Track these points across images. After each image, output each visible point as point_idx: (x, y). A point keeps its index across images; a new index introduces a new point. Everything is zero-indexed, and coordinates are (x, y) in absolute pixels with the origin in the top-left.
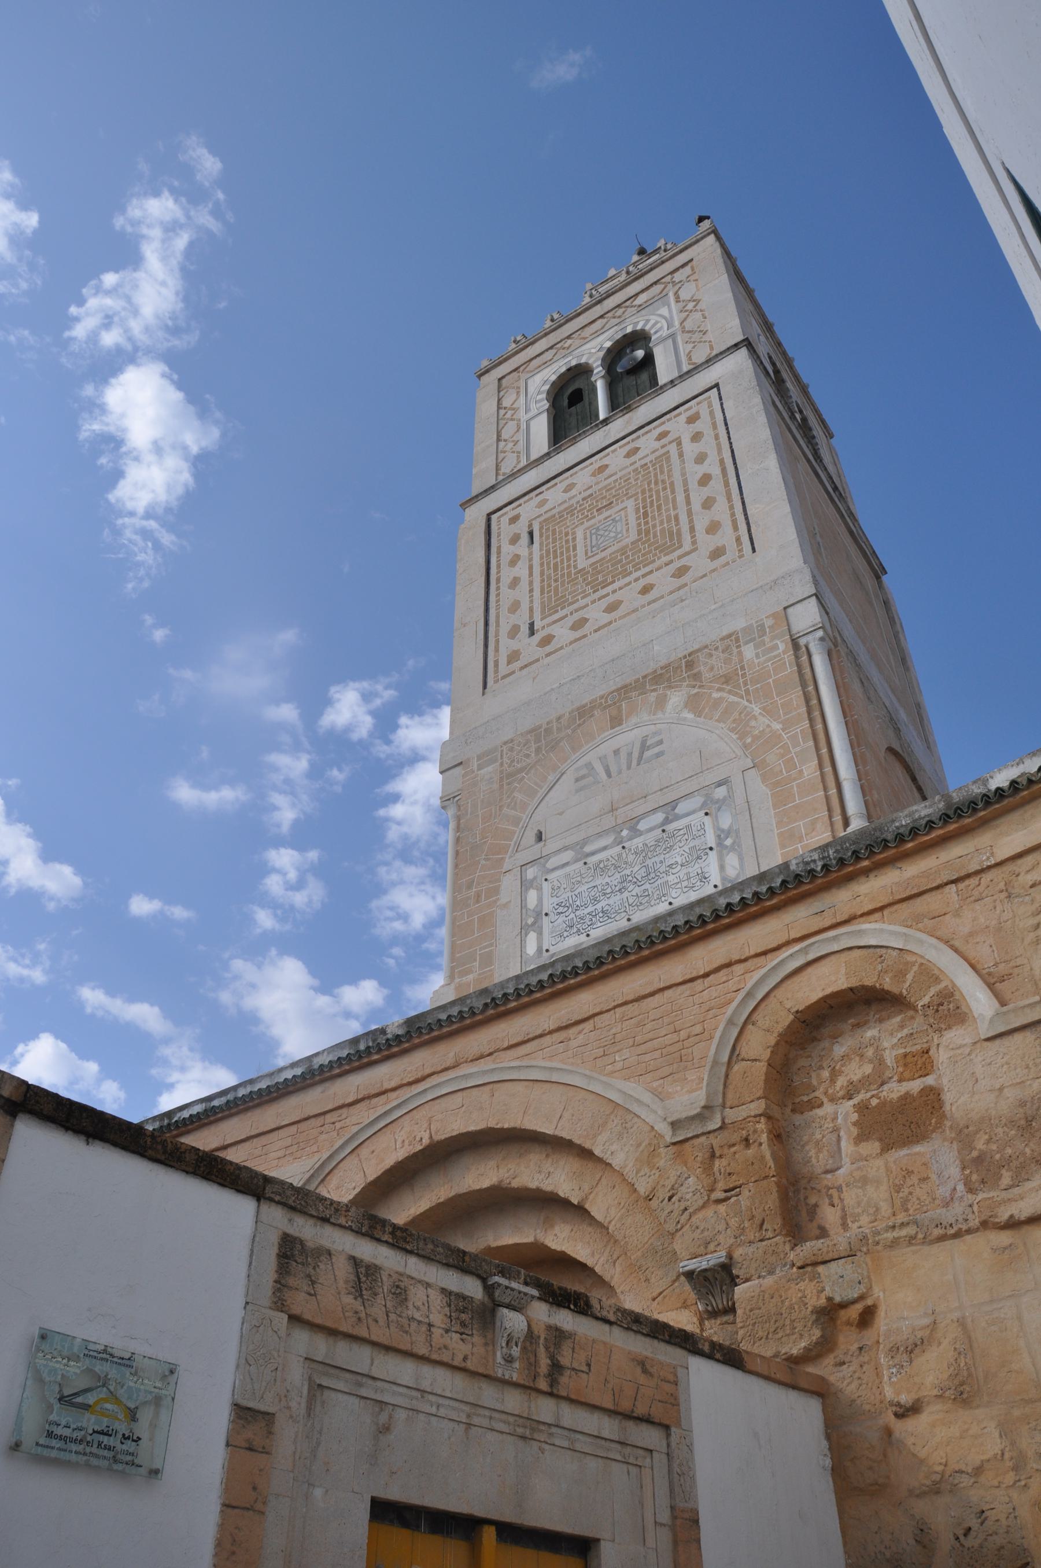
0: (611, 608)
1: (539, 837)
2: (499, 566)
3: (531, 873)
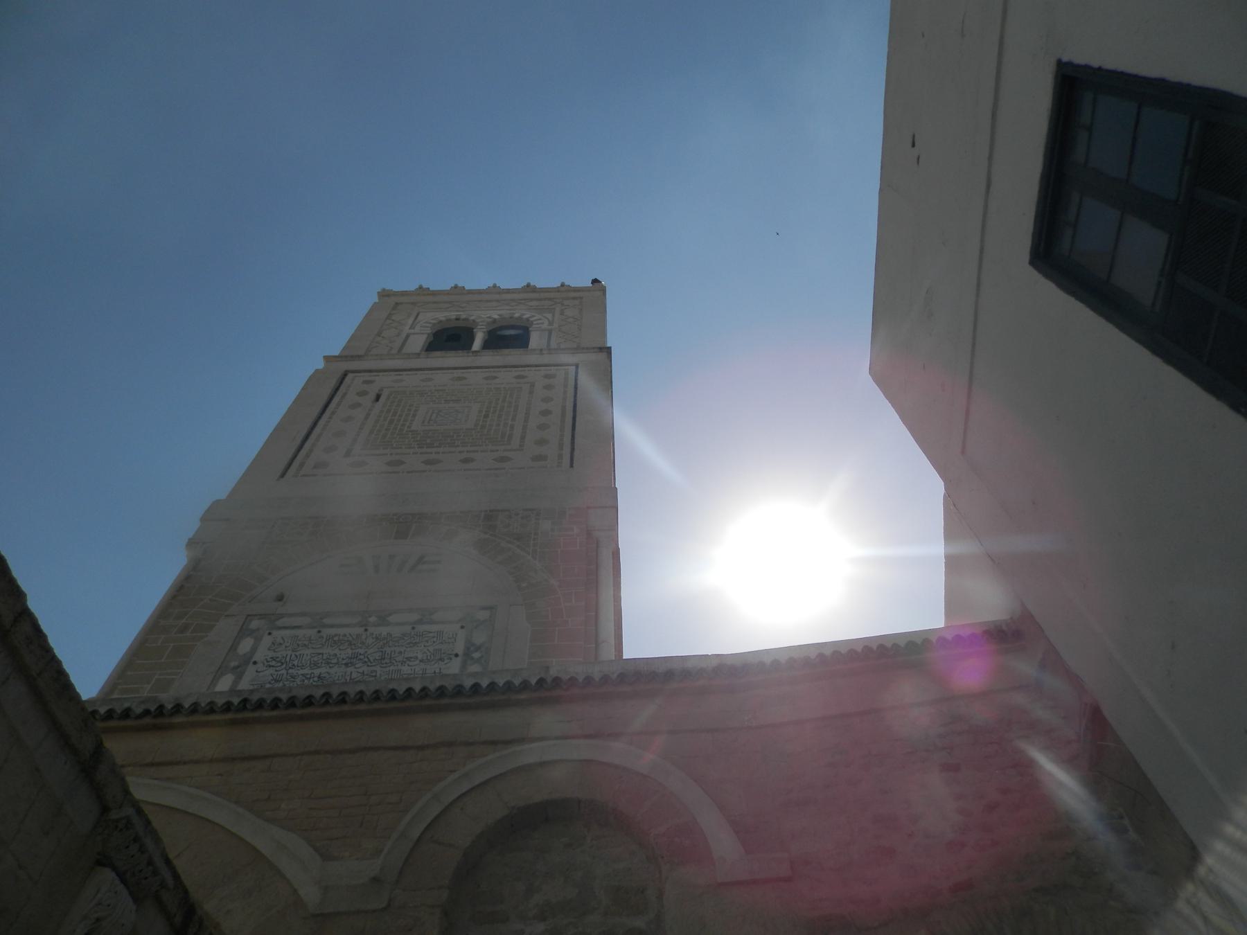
1: (280, 598)
2: (339, 404)
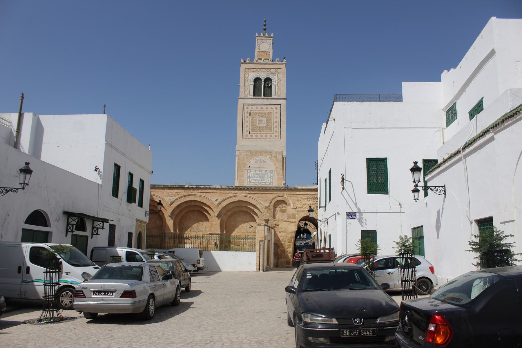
0: (261, 136)
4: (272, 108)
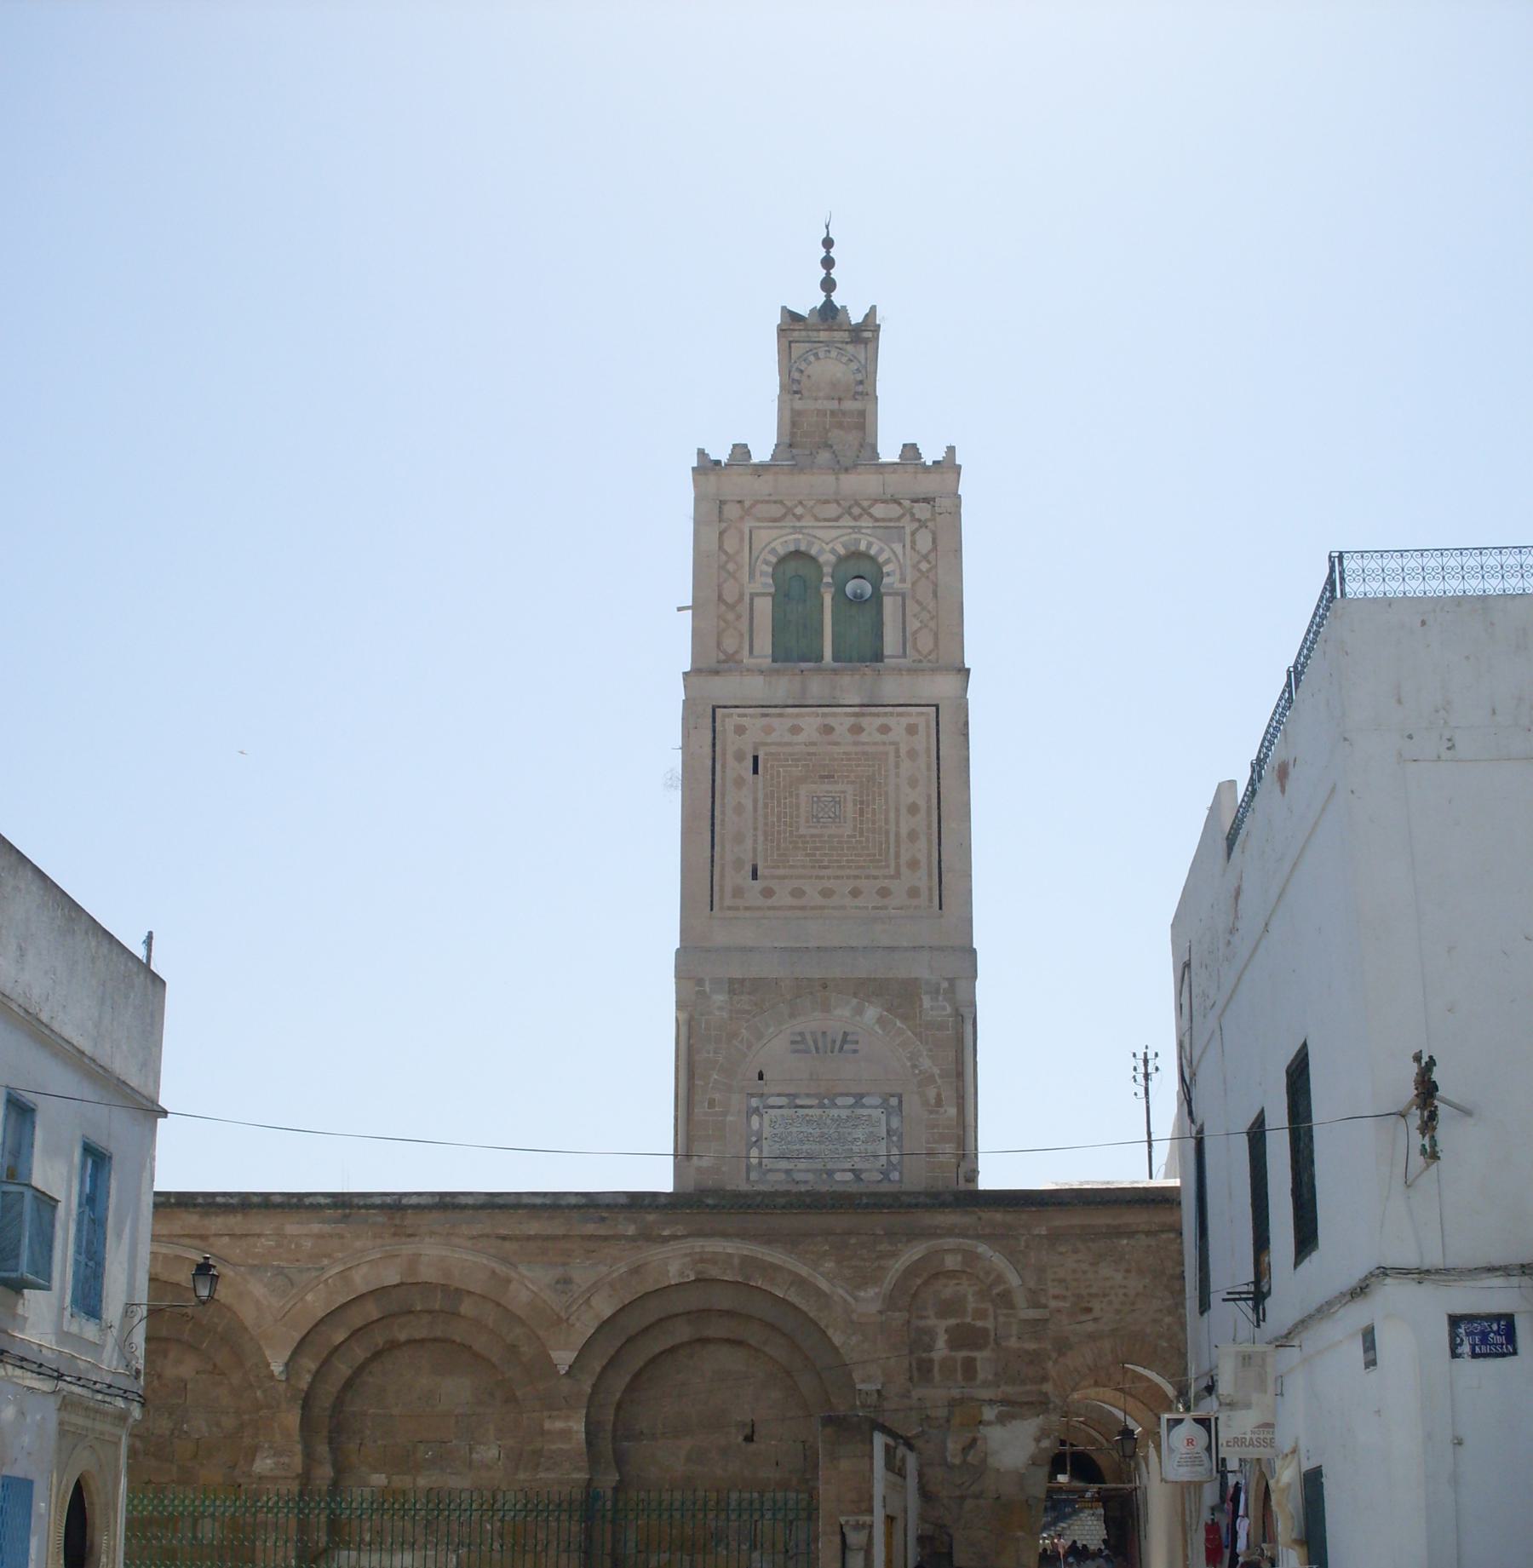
0: (827, 893)
1: (761, 1077)
3: (754, 1102)
4: (885, 729)
